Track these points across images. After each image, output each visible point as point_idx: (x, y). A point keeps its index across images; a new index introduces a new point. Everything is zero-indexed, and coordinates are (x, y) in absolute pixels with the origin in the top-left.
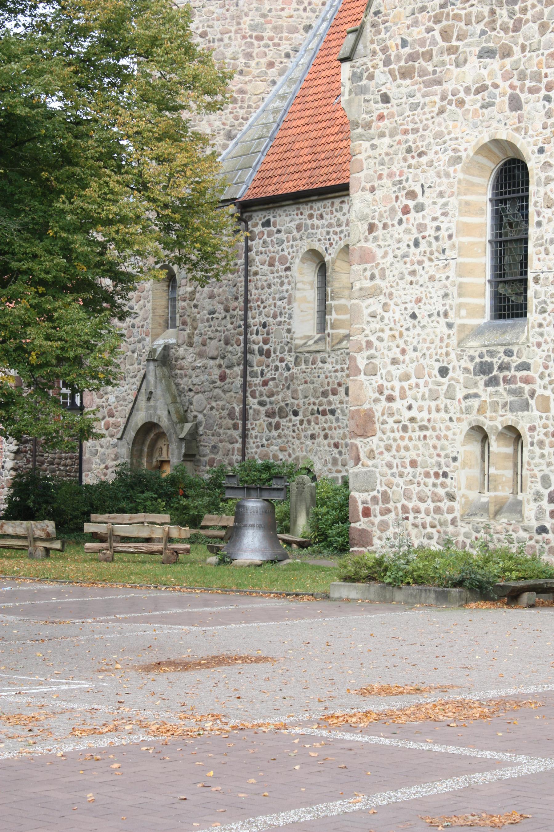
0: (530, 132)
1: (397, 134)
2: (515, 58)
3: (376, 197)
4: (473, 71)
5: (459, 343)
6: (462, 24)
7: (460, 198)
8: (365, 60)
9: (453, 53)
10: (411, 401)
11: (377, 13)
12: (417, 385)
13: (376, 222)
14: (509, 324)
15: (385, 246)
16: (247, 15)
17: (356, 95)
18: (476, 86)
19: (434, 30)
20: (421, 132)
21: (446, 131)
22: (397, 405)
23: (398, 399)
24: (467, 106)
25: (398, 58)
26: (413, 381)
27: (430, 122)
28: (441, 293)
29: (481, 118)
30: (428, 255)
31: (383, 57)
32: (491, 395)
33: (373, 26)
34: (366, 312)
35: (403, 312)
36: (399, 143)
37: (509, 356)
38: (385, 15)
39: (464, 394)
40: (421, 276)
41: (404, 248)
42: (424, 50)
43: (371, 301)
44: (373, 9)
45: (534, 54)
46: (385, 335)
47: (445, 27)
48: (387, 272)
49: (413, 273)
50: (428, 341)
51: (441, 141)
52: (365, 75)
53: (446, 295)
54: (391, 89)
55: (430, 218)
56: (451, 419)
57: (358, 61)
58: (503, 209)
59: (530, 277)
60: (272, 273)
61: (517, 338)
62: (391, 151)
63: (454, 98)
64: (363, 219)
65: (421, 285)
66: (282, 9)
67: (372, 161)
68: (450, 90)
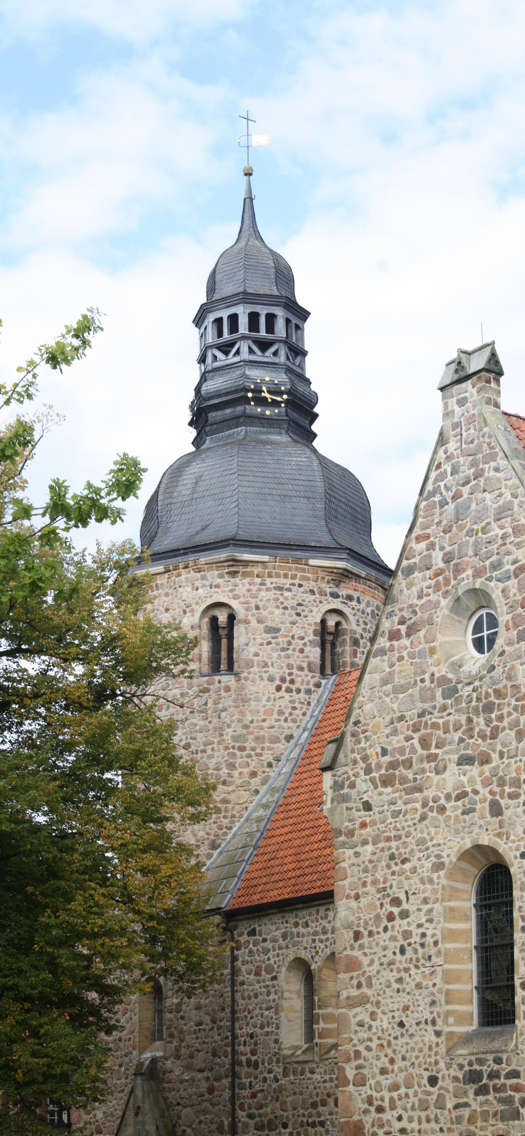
0: (512, 837)
1: (380, 841)
2: (494, 764)
3: (361, 905)
4: (453, 777)
5: (447, 1052)
6: (441, 732)
7: (445, 904)
8: (346, 769)
9: (433, 761)
10: (400, 1111)
11: (356, 723)
12: (407, 1095)
13: (361, 929)
14: (497, 1031)
15: (371, 954)
17: (338, 803)
18: (456, 793)
19: (413, 738)
20: (404, 839)
21: (428, 838)
22: (386, 1116)
23: (388, 1109)
24: (448, 813)
25: (379, 766)
26: (403, 1091)
27: (412, 829)
28: (428, 1000)
29: (462, 824)
30: (414, 962)
31: (364, 766)
32: (481, 1104)
33: (353, 735)
34: (354, 1021)
35: (390, 1020)
36: (382, 850)
37: (499, 1064)
38: (365, 725)
39: (454, 1104)
40: (408, 983)
41: (390, 956)
42: (404, 758)
43: (358, 1009)
44: (352, 720)
45: (512, 761)
46: (373, 1045)
47: (423, 735)
48: (374, 980)
49: (400, 980)
50: (416, 1050)
51: (423, 848)
52: (347, 783)
53: (433, 1003)
54: (371, 796)
55: (415, 925)
56: (441, 1130)
57: (341, 770)
58: (487, 914)
59: (517, 982)
60: (259, 982)
61: (506, 1046)
62: (375, 858)
63: (435, 805)
64: (348, 926)
65: (408, 993)
67: (355, 869)
68: (431, 796)
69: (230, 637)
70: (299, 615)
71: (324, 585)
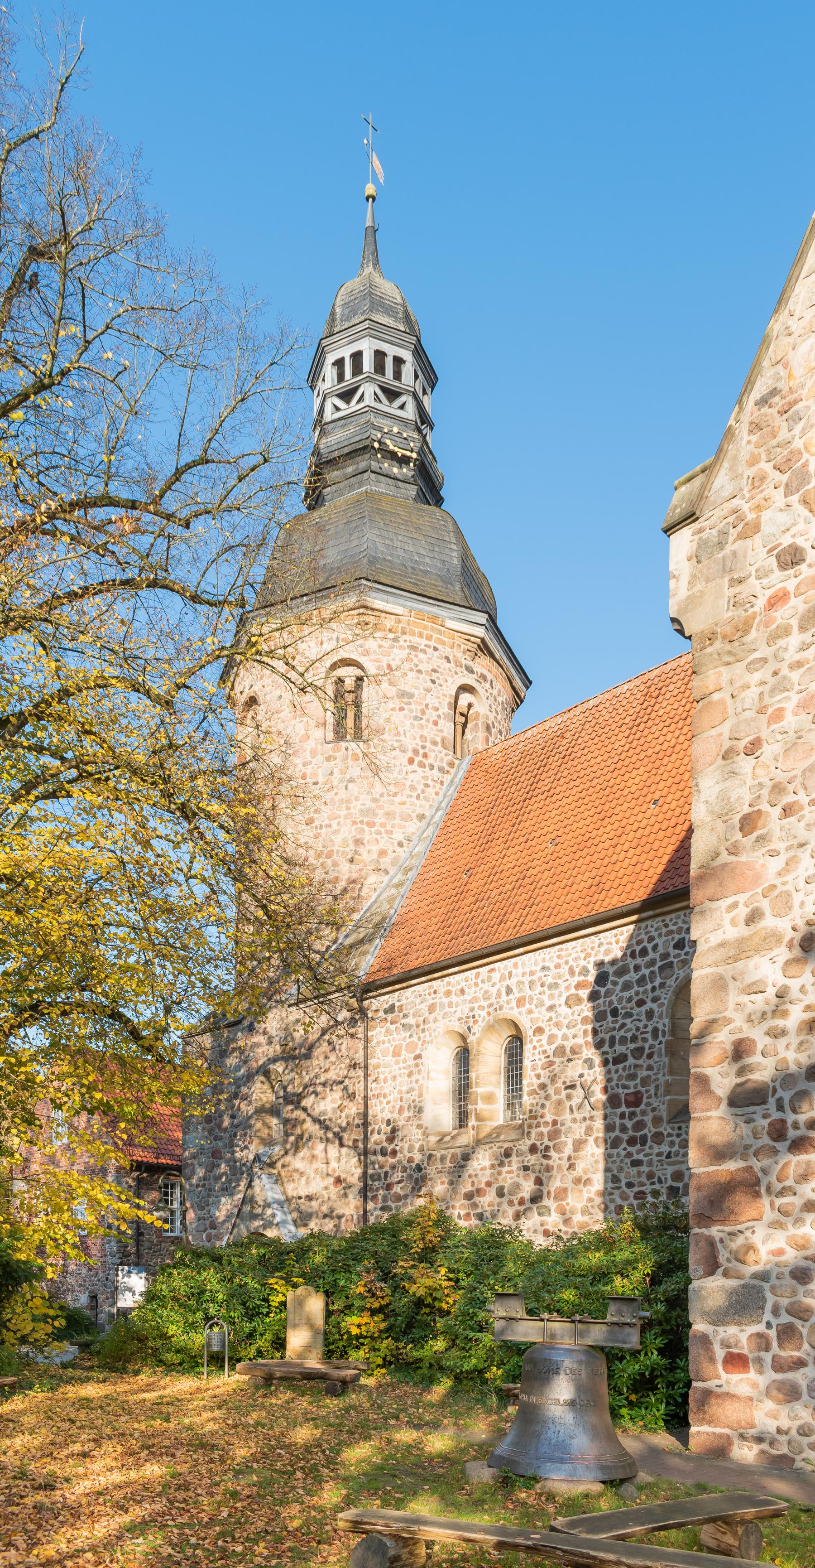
16: (357, 799)
60: (397, 1063)
69: (357, 705)
70: (433, 682)
71: (460, 655)
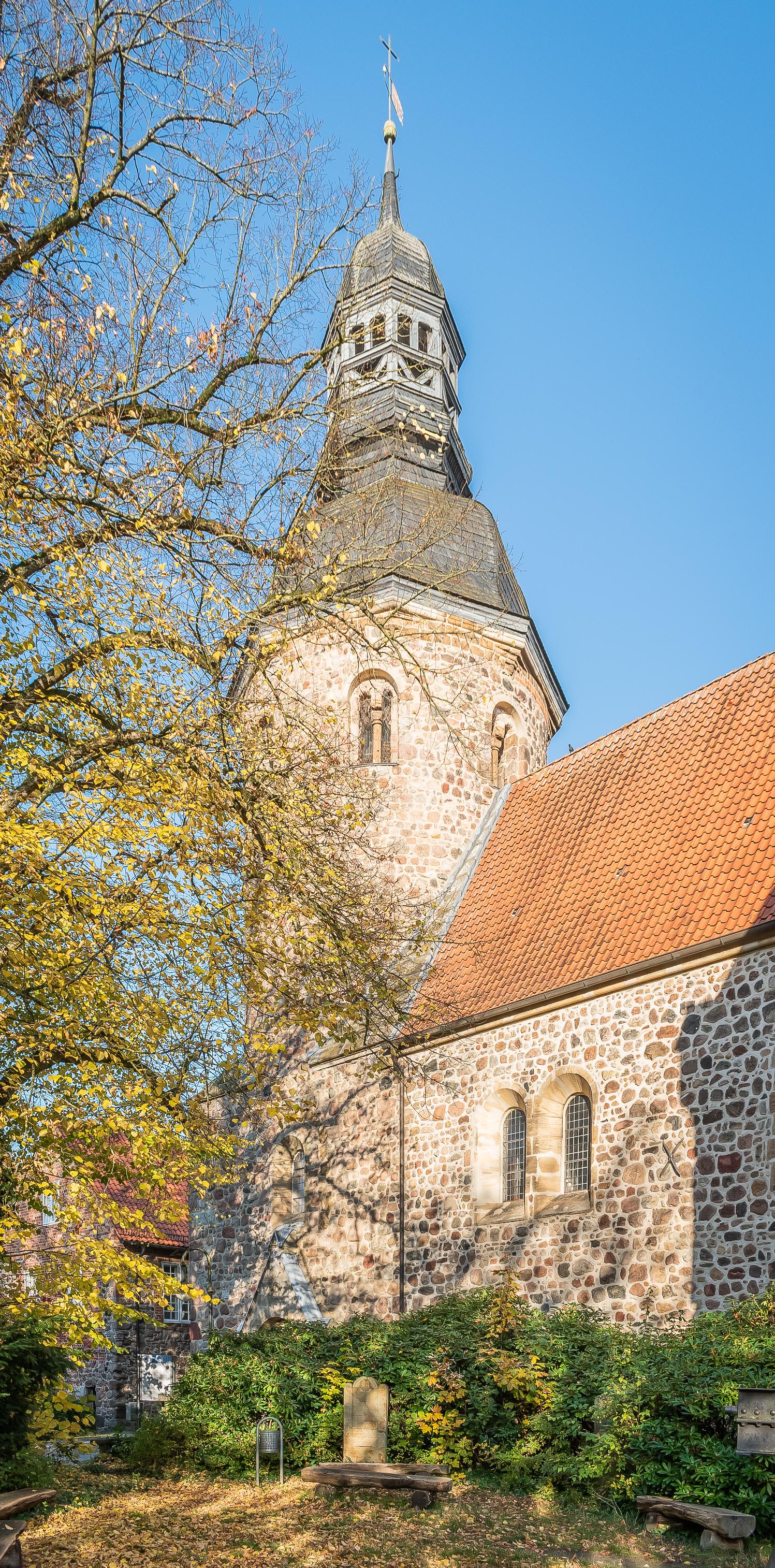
66: (428, 827)
71: (498, 668)
